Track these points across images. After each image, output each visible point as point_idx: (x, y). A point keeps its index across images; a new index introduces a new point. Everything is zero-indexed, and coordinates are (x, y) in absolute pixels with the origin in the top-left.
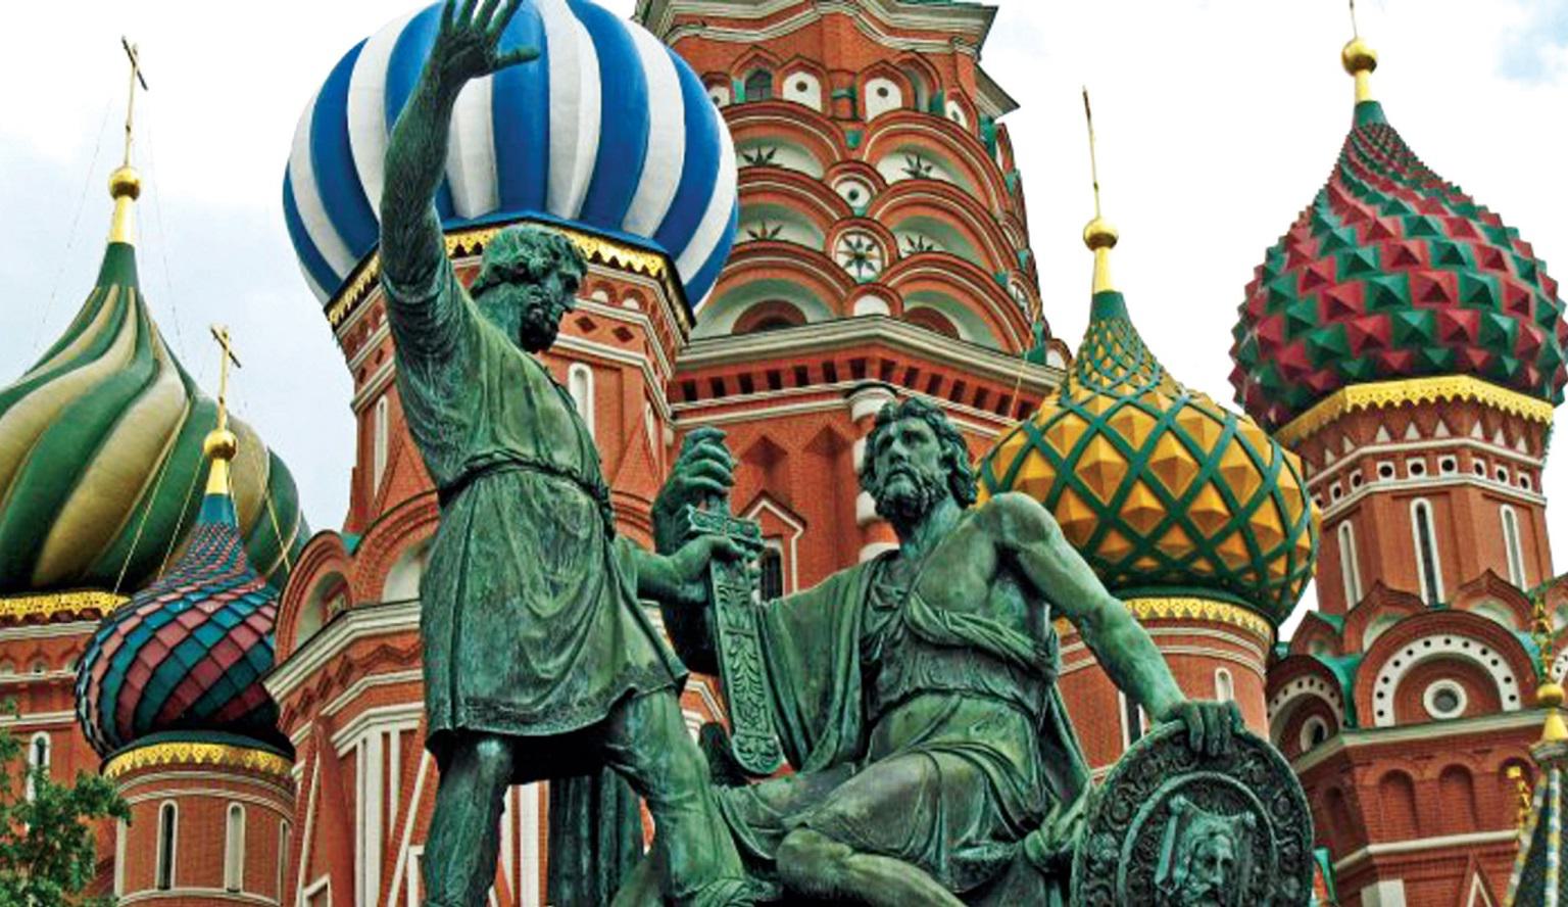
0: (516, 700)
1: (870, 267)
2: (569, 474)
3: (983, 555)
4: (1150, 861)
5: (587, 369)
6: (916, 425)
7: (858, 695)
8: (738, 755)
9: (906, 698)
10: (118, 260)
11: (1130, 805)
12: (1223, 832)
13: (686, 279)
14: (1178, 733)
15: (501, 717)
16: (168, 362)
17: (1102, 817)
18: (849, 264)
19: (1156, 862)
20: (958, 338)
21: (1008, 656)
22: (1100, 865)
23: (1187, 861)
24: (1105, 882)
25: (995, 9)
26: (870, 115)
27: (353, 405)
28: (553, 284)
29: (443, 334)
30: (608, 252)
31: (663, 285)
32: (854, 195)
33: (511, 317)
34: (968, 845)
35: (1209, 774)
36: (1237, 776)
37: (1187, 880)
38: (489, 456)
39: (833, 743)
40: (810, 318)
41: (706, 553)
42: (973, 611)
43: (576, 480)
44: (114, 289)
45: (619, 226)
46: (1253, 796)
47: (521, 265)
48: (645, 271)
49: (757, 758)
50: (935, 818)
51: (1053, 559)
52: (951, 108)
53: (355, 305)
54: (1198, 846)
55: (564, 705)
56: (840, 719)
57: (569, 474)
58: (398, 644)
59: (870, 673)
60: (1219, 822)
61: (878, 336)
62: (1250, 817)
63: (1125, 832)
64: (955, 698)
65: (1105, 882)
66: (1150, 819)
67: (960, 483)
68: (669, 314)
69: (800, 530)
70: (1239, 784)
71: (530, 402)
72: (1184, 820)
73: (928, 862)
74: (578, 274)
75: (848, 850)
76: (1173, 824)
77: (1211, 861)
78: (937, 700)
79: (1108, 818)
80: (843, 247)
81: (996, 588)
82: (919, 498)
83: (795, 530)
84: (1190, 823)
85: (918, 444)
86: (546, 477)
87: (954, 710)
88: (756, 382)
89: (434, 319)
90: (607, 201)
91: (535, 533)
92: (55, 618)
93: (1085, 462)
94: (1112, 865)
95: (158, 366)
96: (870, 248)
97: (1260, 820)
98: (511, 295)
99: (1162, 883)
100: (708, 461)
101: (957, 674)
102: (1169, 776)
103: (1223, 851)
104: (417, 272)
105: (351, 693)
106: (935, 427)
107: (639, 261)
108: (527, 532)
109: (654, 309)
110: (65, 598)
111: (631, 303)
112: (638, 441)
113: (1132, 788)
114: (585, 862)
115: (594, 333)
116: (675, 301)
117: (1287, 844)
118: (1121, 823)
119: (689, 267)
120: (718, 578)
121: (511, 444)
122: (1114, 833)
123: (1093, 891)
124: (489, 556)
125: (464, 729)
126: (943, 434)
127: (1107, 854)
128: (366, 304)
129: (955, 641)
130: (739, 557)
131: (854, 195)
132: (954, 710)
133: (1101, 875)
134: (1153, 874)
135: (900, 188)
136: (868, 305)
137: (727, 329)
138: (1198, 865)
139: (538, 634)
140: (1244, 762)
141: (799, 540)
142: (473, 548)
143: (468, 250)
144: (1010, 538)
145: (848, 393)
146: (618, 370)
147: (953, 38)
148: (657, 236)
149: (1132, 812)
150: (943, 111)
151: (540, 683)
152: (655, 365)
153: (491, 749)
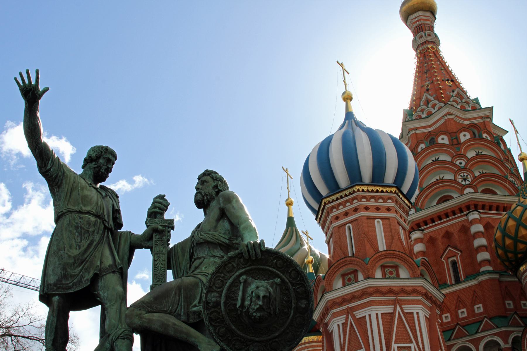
0: (64, 282)
1: (468, 181)
2: (88, 213)
4: (234, 300)
6: (205, 178)
10: (290, 222)
11: (222, 281)
12: (262, 286)
13: (405, 192)
15: (59, 288)
17: (210, 287)
18: (462, 181)
19: (237, 300)
20: (497, 194)
21: (218, 243)
22: (212, 304)
23: (249, 298)
24: (216, 309)
25: (493, 107)
26: (462, 141)
28: (101, 161)
29: (57, 180)
30: (380, 189)
31: (398, 194)
32: (461, 163)
33: (90, 173)
34: (195, 306)
35: (256, 267)
36: (270, 266)
37: (250, 305)
38: (62, 211)
42: (209, 231)
44: (290, 228)
45: (383, 182)
46: (279, 273)
47: (90, 157)
48: (391, 192)
50: (179, 298)
52: (485, 136)
53: (321, 216)
54: (252, 292)
55: (80, 281)
57: (88, 213)
58: (338, 301)
60: (264, 283)
61: (472, 198)
63: (223, 290)
64: (202, 259)
65: (216, 309)
68: (402, 202)
69: (460, 253)
70: (271, 269)
71: (79, 194)
72: (246, 284)
73: (178, 314)
74: (110, 157)
75: (144, 312)
77: (258, 297)
79: (214, 288)
80: (460, 177)
81: (221, 222)
82: (203, 200)
84: (250, 284)
85: (205, 184)
86: (79, 214)
87: (201, 263)
88: (442, 217)
89: (52, 176)
90: (378, 177)
91: (75, 231)
93: (523, 219)
94: (217, 304)
96: (467, 176)
97: (283, 280)
98: (90, 167)
99: (239, 307)
101: (202, 252)
102: (239, 269)
103: (262, 294)
104: (45, 163)
105: (329, 316)
106: (212, 178)
107: (389, 190)
108: (71, 232)
109: (396, 201)
111: (390, 201)
113: (222, 275)
115: (380, 211)
116: (403, 198)
117: (298, 288)
118: (219, 288)
119: (405, 189)
120: (156, 237)
121: (70, 207)
122: (218, 292)
123: (211, 313)
124: (57, 240)
125: (46, 294)
127: (214, 299)
128: (323, 215)
129: (201, 241)
131: (461, 163)
132: (201, 263)
133: (214, 307)
134: (236, 304)
135: (473, 158)
136: (468, 190)
138: (254, 299)
139: (71, 261)
140: (272, 261)
142: (53, 240)
144: (222, 205)
145: (466, 215)
146: (389, 219)
147: (482, 117)
148: (394, 183)
149: (223, 284)
150: (482, 137)
151: (72, 276)
152: (401, 216)
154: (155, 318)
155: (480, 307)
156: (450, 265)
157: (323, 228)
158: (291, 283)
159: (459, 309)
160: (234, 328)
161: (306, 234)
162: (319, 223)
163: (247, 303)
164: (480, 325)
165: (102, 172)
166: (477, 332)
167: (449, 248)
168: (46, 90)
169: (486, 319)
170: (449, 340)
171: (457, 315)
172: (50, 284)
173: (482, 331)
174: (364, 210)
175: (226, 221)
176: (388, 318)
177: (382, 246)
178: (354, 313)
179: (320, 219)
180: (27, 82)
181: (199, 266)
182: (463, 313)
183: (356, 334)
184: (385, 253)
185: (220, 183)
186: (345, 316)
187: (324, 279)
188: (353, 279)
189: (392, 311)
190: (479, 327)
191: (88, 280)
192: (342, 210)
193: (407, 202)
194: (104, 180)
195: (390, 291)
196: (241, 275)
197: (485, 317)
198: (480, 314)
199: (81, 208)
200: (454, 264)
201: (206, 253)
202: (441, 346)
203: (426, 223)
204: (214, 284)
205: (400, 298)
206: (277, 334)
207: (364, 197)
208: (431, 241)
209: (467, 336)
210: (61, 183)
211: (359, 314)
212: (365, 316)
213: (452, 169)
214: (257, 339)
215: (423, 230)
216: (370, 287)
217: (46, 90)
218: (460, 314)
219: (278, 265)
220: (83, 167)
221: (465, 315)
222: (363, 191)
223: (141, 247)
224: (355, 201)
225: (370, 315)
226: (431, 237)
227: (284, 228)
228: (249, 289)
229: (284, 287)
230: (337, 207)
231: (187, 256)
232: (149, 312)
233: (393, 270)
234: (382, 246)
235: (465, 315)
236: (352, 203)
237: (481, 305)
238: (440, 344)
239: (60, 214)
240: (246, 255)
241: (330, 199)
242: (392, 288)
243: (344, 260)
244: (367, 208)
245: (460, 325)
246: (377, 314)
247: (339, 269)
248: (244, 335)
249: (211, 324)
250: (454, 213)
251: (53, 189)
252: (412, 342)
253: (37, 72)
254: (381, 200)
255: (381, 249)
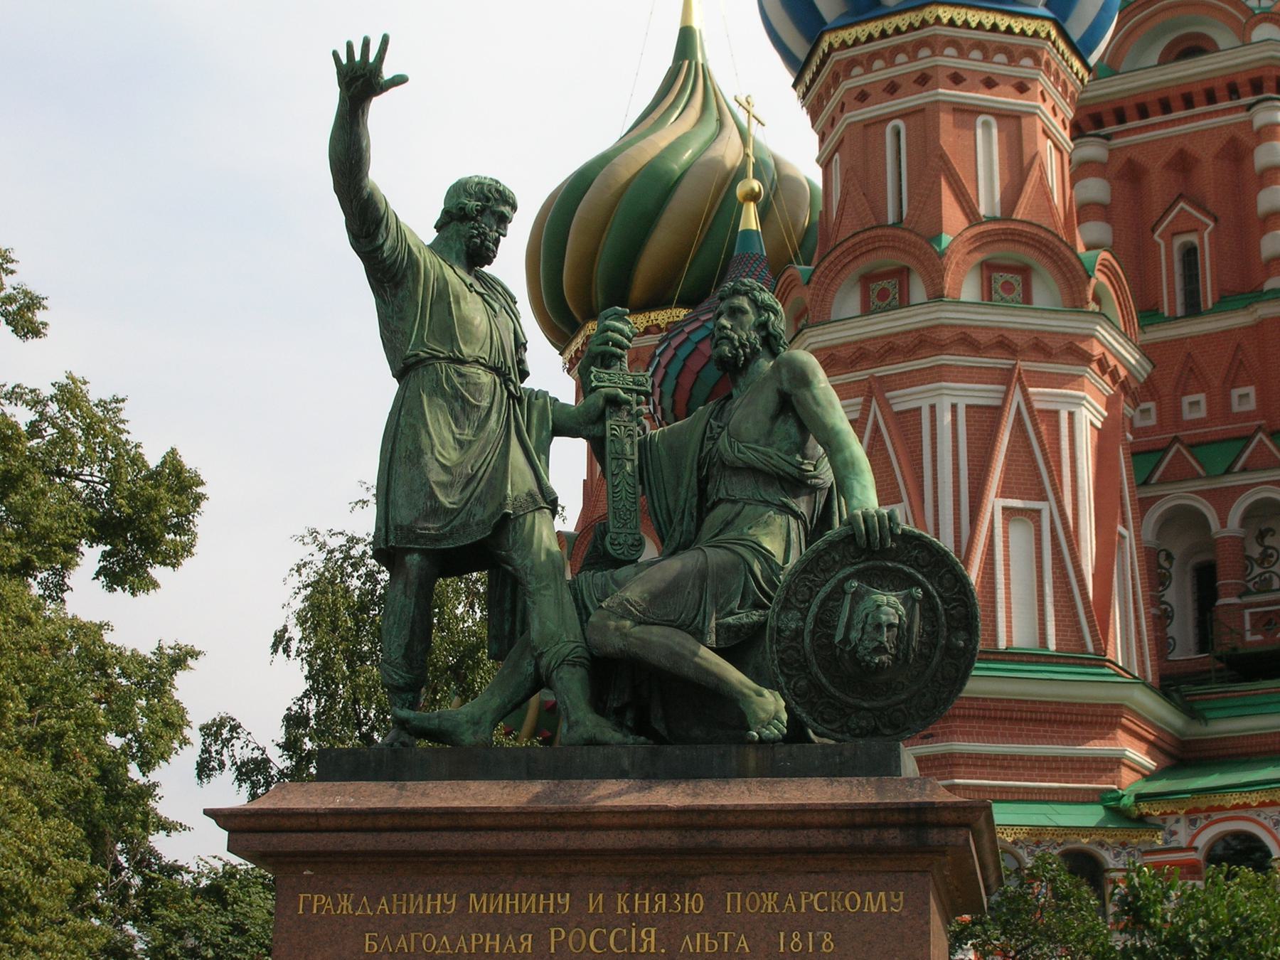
3: (767, 400)
4: (829, 627)
5: (992, 120)
7: (695, 500)
8: (609, 547)
9: (715, 505)
10: (686, 42)
11: (810, 588)
13: (1076, 36)
14: (848, 536)
16: (729, 121)
17: (787, 600)
19: (835, 627)
22: (788, 633)
24: (794, 644)
27: (818, 161)
33: (458, 246)
34: (731, 613)
35: (878, 563)
36: (904, 563)
38: (417, 355)
39: (677, 535)
40: (1222, 45)
41: (601, 402)
42: (757, 442)
43: (482, 364)
46: (920, 577)
49: (625, 549)
51: (811, 401)
53: (813, 81)
54: (867, 616)
56: (683, 518)
58: (844, 353)
59: (703, 483)
61: (1272, 58)
62: (919, 593)
64: (740, 505)
65: (794, 644)
66: (829, 597)
67: (772, 341)
69: (1212, 225)
70: (905, 568)
72: (858, 597)
76: (848, 598)
78: (729, 505)
79: (793, 600)
82: (736, 357)
83: (1207, 226)
84: (862, 597)
87: (738, 514)
92: (647, 331)
94: (799, 633)
95: (721, 124)
97: (926, 591)
100: (610, 333)
102: (843, 567)
106: (754, 301)
109: (1048, 64)
110: (653, 315)
112: (1034, 174)
114: (507, 627)
116: (1067, 53)
118: (803, 602)
122: (800, 610)
123: (784, 651)
126: (760, 307)
129: (740, 464)
130: (628, 402)
132: (738, 514)
134: (833, 636)
137: (1154, 58)
138: (869, 629)
139: (444, 478)
141: (1210, 234)
143: (890, 32)
144: (786, 386)
145: (1249, 107)
149: (812, 595)
152: (1053, 108)
153: (414, 560)
154: (655, 639)
155: (1247, 395)
156: (1177, 257)
157: (814, 113)
158: (941, 597)
159: (1185, 394)
160: (824, 680)
161: (747, 106)
162: (804, 98)
163: (855, 635)
164: (1242, 451)
165: (488, 248)
166: (1228, 471)
167: (1182, 204)
168: (399, 80)
169: (1260, 436)
170: (1146, 483)
171: (1178, 410)
172: (401, 527)
173: (1244, 469)
174: (949, 82)
175: (791, 421)
176: (984, 422)
177: (988, 201)
178: (888, 395)
179: (808, 89)
180: (358, 57)
181: (733, 520)
182: (1195, 407)
183: (888, 457)
184: (996, 226)
185: (773, 317)
186: (860, 400)
187: (808, 283)
188: (894, 292)
189: (998, 403)
190: (1239, 456)
191: (483, 522)
192: (881, 73)
193: (1077, 64)
194: (489, 263)
195: (1004, 344)
196: (847, 578)
197: (1259, 428)
198: (1247, 416)
199: (460, 352)
200: (1190, 254)
201: (750, 494)
202: (1123, 513)
203: (1121, 117)
204: (795, 594)
205: (1023, 365)
206: (904, 697)
207: (953, 42)
208: (1129, 174)
209: (1199, 477)
210: (404, 276)
211: (903, 400)
212: (919, 409)
213: (1235, 17)
214: (866, 705)
215: (1108, 137)
216: (943, 326)
217: (399, 80)
218: (1185, 407)
219: (920, 561)
220: (439, 227)
221: (1202, 413)
222: (952, 23)
223: (574, 434)
224: (925, 52)
225: (933, 407)
226: (1130, 161)
227: (667, 61)
228: (861, 608)
229: (927, 606)
230: (867, 62)
231: (689, 478)
232: (640, 623)
233: (1016, 279)
234: (988, 201)
235: (1202, 413)
236: (913, 57)
237: (1251, 390)
238: (1123, 506)
239: (413, 360)
240: (862, 542)
241: (848, 35)
242: (1006, 334)
243: (873, 233)
244: (957, 79)
245: (1182, 443)
246: (954, 407)
247: (856, 258)
248: (842, 696)
249: (782, 672)
250: (1211, 98)
251: (384, 288)
252: (1045, 499)
253: (385, 41)
254: (1001, 58)
255: (983, 210)
